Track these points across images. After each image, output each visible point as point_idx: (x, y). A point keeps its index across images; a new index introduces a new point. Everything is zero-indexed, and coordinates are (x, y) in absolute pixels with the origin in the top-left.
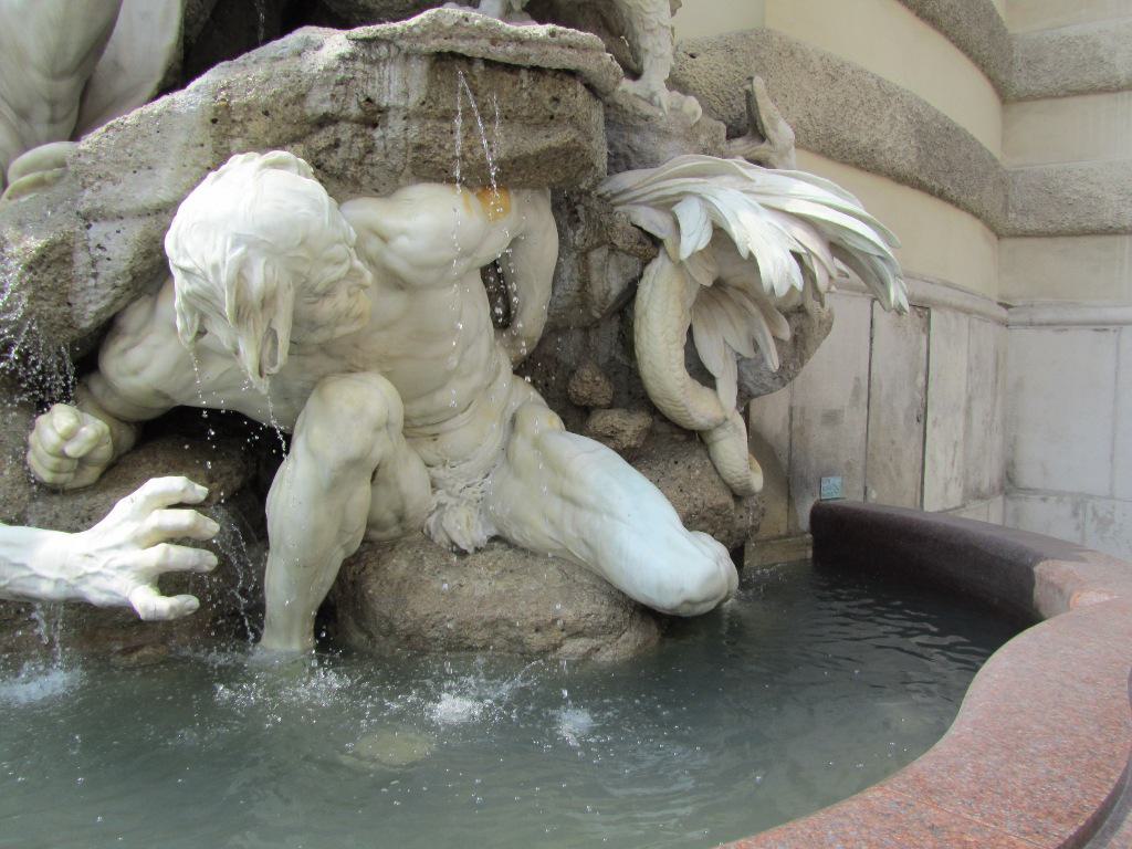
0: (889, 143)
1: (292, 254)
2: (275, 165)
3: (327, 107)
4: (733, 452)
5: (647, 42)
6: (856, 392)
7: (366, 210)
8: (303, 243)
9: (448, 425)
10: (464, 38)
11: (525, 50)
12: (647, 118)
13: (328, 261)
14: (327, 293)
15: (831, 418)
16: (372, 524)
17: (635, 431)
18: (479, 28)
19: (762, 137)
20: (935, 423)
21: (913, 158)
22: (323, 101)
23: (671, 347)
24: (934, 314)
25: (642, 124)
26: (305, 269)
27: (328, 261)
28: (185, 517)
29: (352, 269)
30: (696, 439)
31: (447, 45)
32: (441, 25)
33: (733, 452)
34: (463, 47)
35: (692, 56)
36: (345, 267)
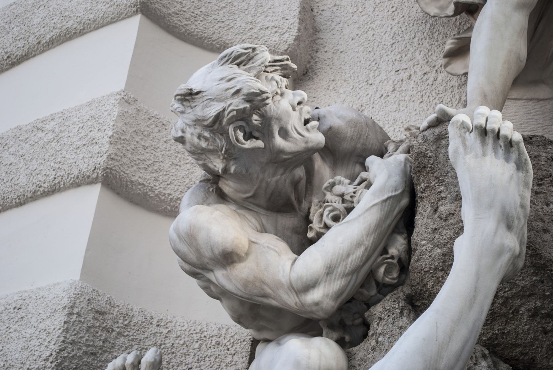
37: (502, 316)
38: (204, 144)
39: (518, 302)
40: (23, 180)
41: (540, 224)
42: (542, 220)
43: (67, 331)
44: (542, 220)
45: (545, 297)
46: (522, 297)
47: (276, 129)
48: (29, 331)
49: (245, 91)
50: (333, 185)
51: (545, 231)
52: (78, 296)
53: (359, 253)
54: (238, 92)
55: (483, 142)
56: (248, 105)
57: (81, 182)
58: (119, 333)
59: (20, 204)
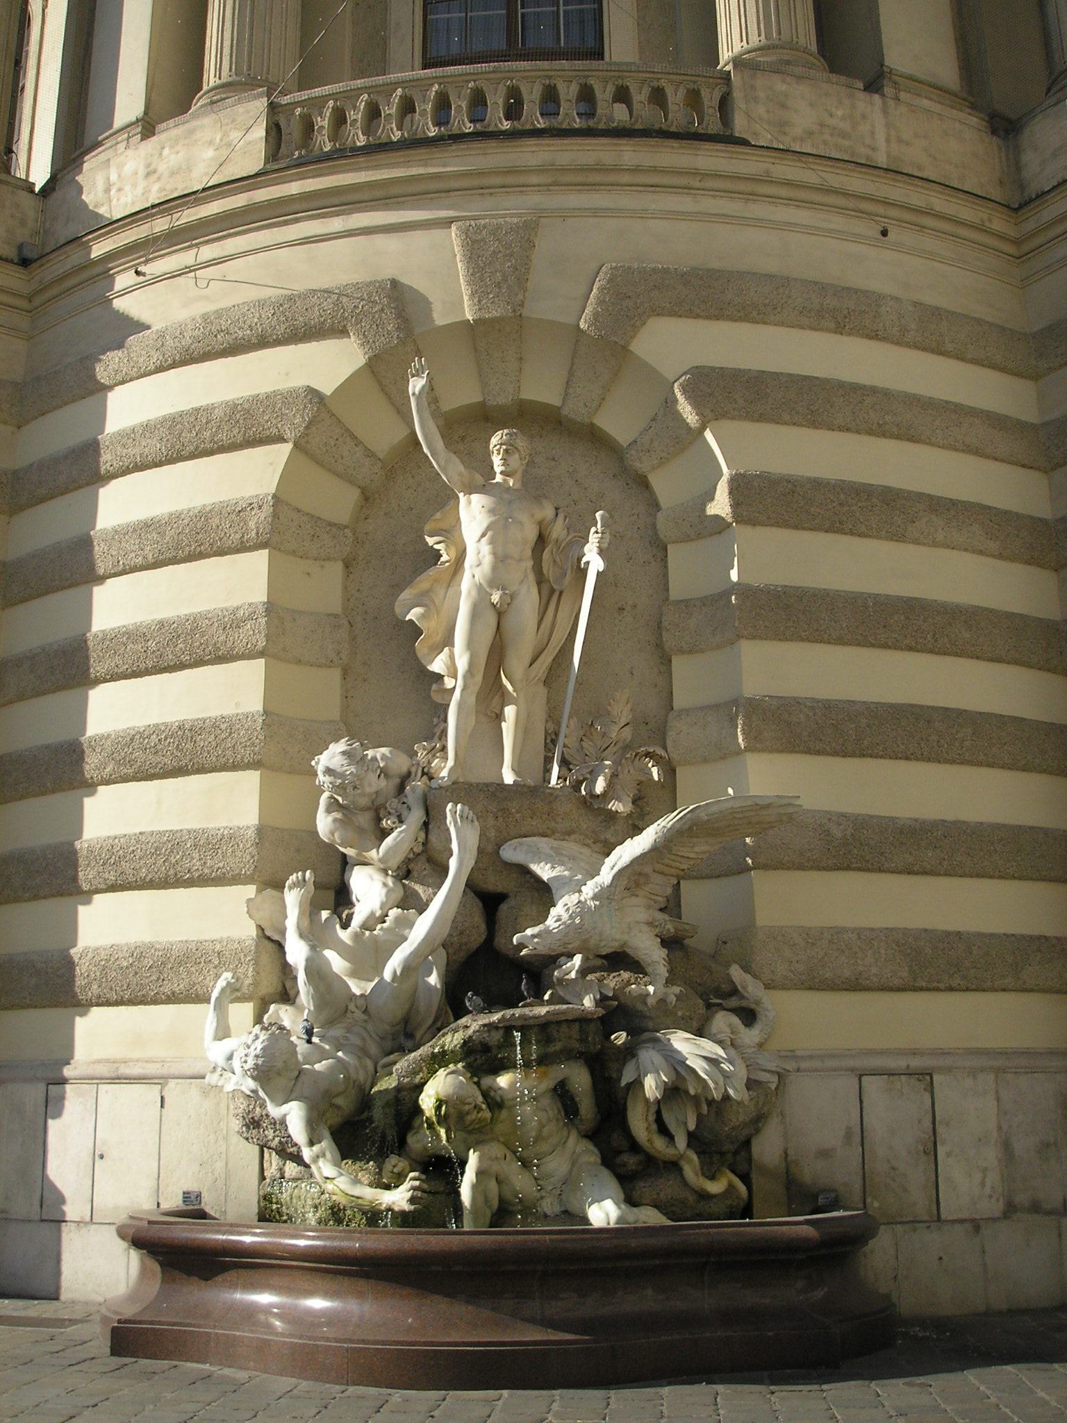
0: (874, 970)
4: (691, 1169)
6: (848, 1136)
7: (486, 1081)
14: (468, 1113)
15: (825, 1154)
16: (502, 1200)
19: (743, 997)
20: (949, 1155)
21: (905, 974)
24: (937, 1078)
28: (417, 1183)
30: (674, 1166)
31: (508, 1024)
33: (691, 1169)
35: (725, 943)
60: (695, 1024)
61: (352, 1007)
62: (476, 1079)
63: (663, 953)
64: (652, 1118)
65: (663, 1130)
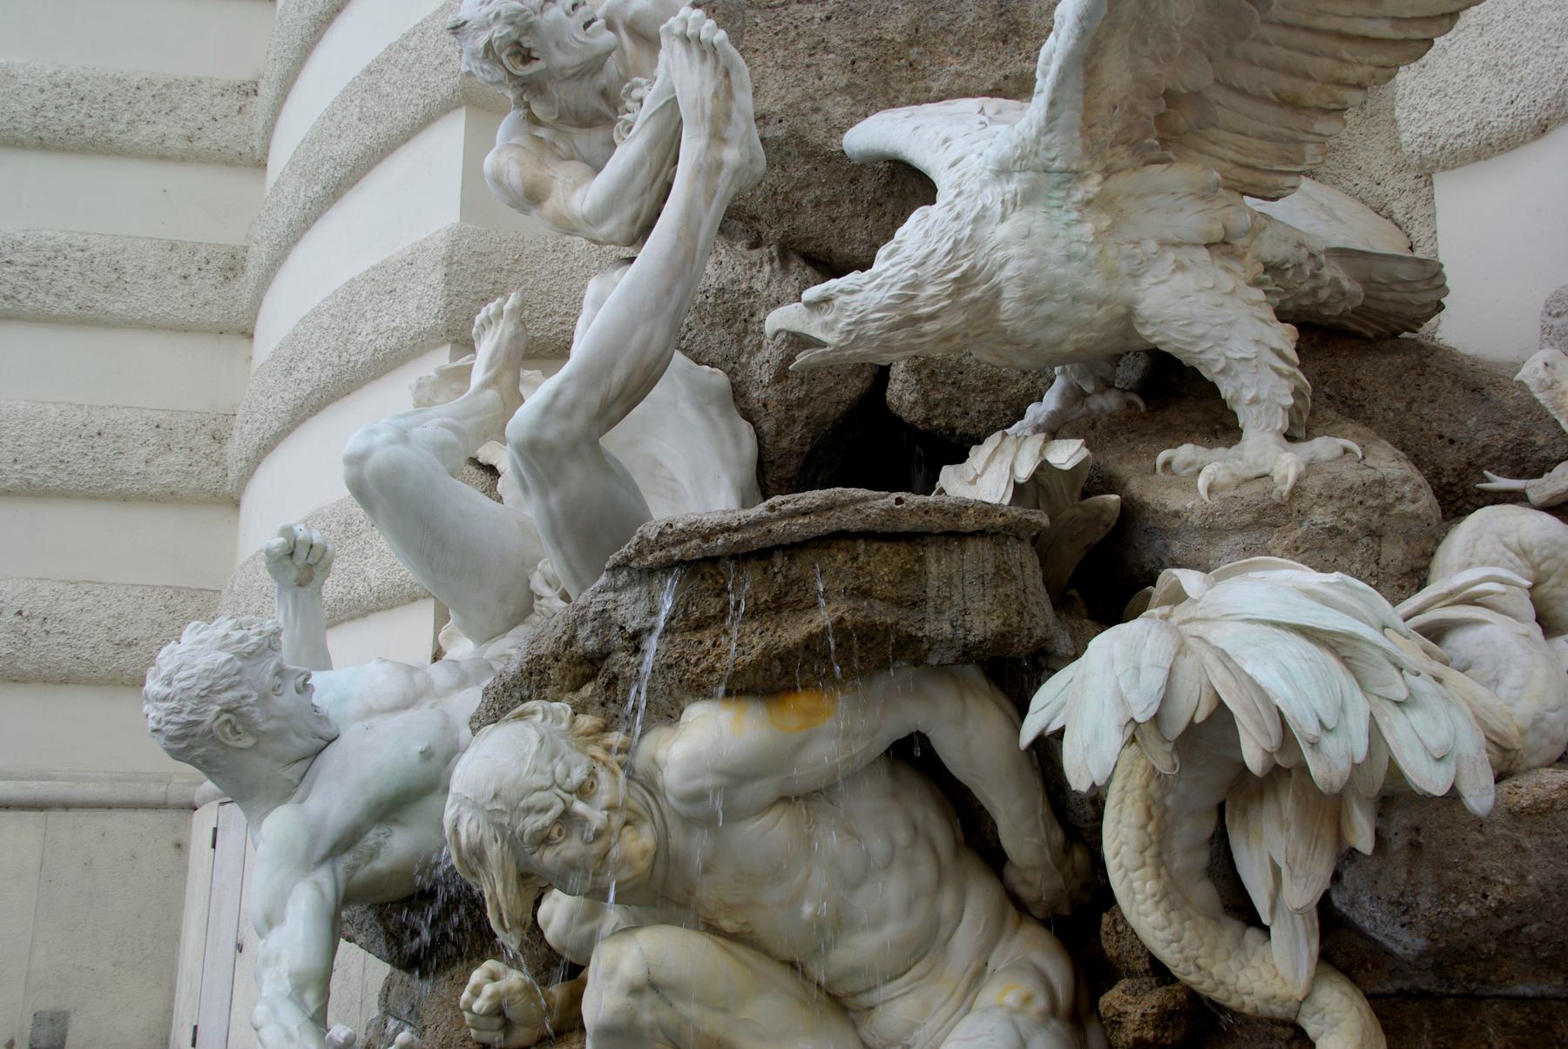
1: (489, 808)
2: (521, 716)
3: (592, 644)
5: (1226, 389)
8: (495, 796)
9: (876, 996)
10: (674, 544)
11: (737, 537)
12: (1177, 514)
13: (528, 810)
17: (1143, 1015)
18: (683, 531)
22: (588, 639)
23: (1131, 875)
25: (1177, 523)
26: (506, 821)
27: (528, 810)
29: (567, 817)
32: (649, 541)
34: (676, 552)
36: (551, 814)
37: (788, 211)
38: (488, 78)
39: (798, 195)
40: (399, 114)
41: (809, 104)
42: (813, 99)
43: (448, 283)
44: (813, 99)
45: (823, 185)
46: (801, 189)
47: (552, 45)
48: (421, 288)
49: (503, 14)
50: (631, 89)
51: (816, 110)
52: (455, 244)
53: (644, 171)
54: (498, 15)
55: (689, 51)
56: (509, 29)
57: (447, 107)
58: (510, 271)
59: (406, 140)
60: (1394, 553)
61: (537, 583)
62: (616, 738)
63: (1284, 337)
64: (1189, 858)
65: (1240, 908)
